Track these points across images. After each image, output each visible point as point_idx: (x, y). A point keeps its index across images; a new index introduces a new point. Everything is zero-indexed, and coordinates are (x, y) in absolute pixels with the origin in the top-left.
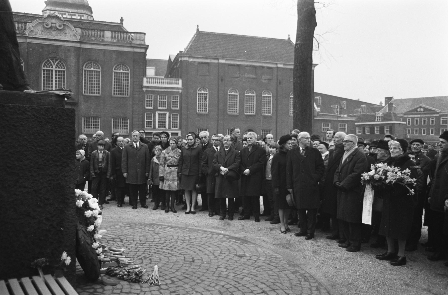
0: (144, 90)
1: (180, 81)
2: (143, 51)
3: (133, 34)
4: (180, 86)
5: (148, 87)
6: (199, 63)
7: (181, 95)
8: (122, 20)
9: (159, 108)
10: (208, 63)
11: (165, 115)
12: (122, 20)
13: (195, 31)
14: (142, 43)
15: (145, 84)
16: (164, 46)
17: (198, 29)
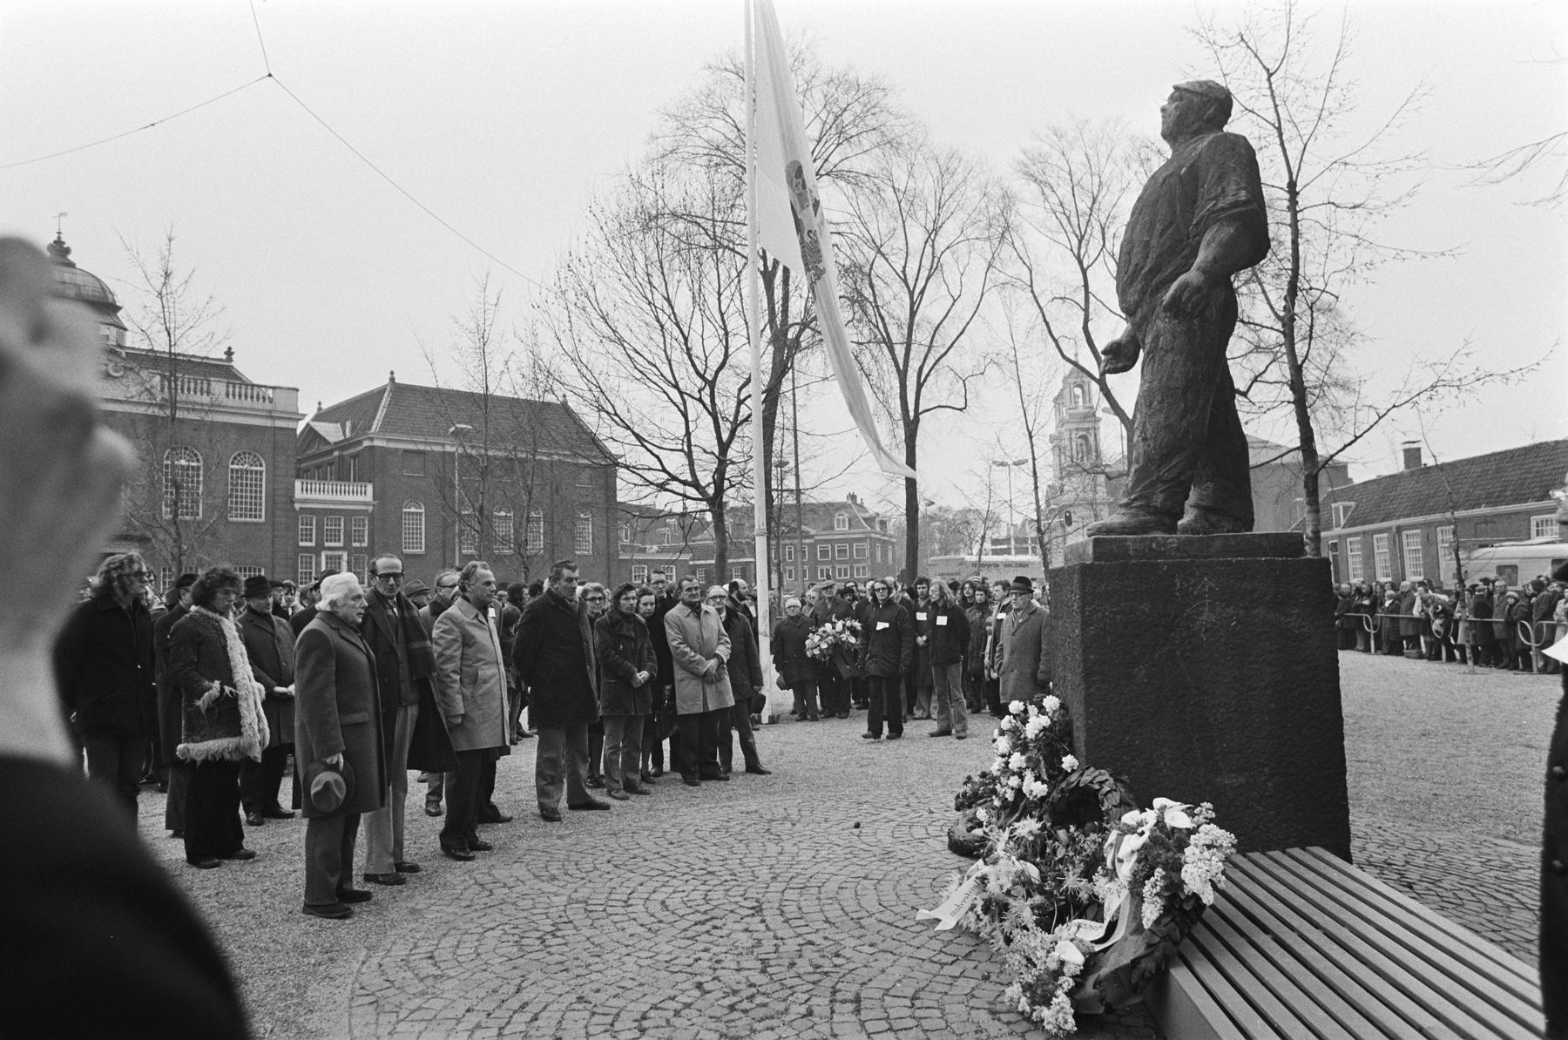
0: (297, 506)
1: (370, 488)
2: (291, 425)
3: (270, 392)
4: (369, 497)
5: (305, 501)
6: (406, 451)
7: (372, 516)
8: (229, 353)
9: (327, 544)
10: (423, 453)
11: (340, 558)
12: (229, 353)
13: (386, 381)
14: (291, 409)
15: (298, 494)
16: (308, 408)
17: (392, 379)
